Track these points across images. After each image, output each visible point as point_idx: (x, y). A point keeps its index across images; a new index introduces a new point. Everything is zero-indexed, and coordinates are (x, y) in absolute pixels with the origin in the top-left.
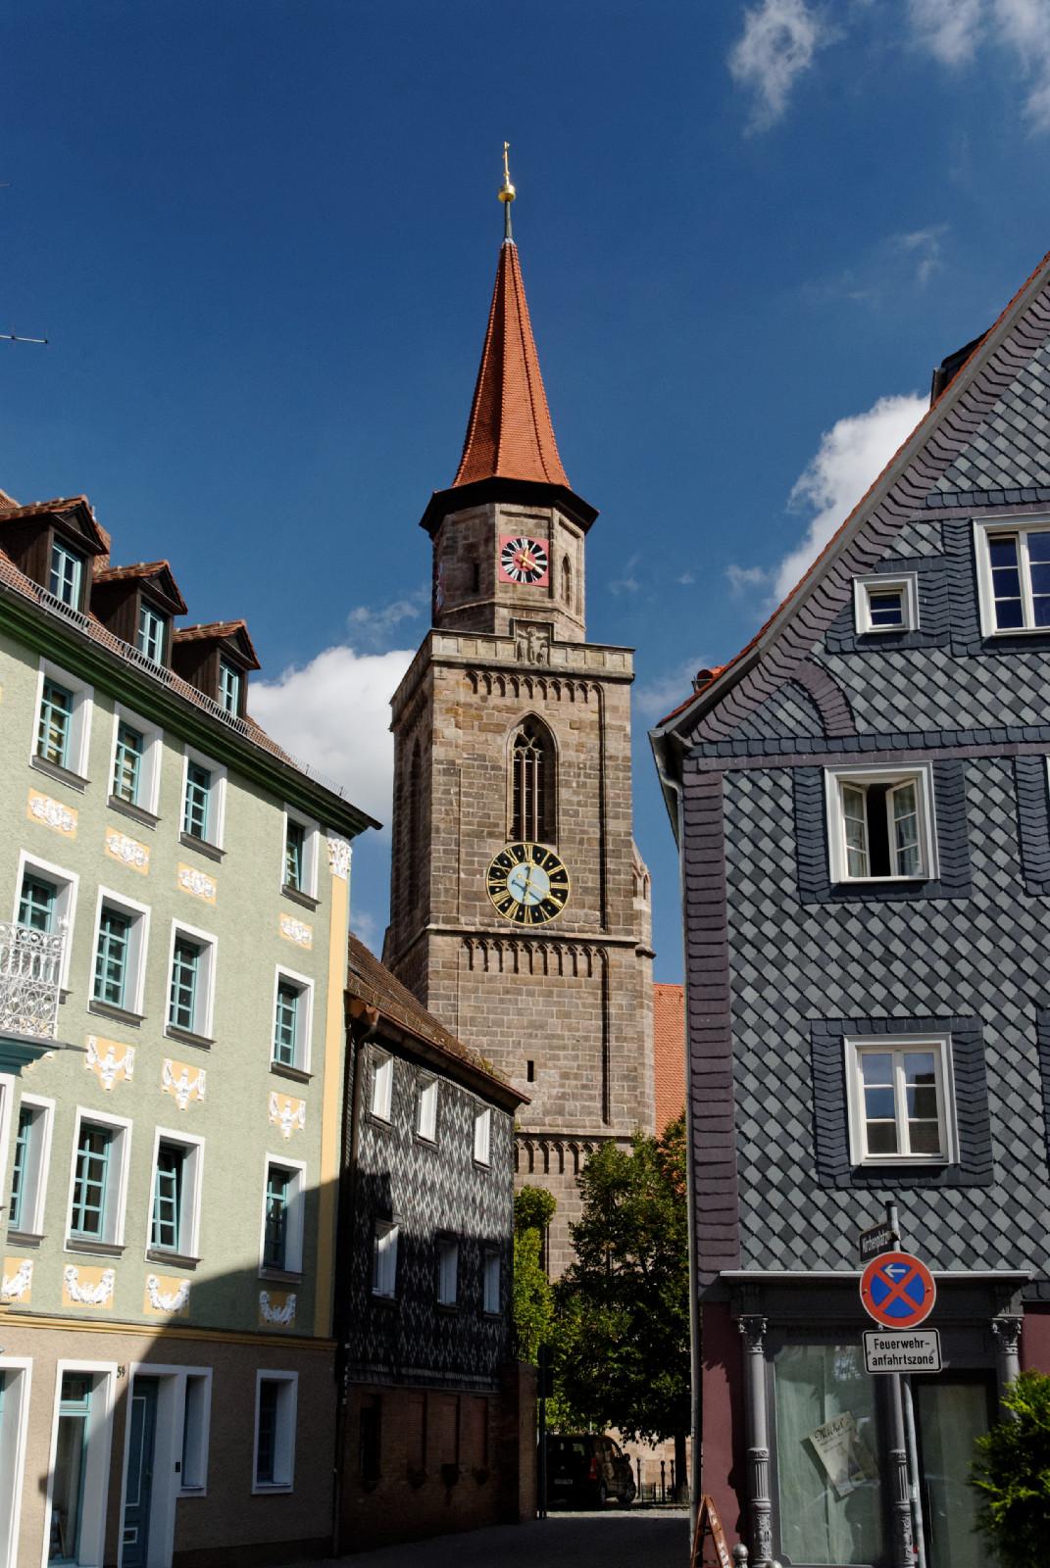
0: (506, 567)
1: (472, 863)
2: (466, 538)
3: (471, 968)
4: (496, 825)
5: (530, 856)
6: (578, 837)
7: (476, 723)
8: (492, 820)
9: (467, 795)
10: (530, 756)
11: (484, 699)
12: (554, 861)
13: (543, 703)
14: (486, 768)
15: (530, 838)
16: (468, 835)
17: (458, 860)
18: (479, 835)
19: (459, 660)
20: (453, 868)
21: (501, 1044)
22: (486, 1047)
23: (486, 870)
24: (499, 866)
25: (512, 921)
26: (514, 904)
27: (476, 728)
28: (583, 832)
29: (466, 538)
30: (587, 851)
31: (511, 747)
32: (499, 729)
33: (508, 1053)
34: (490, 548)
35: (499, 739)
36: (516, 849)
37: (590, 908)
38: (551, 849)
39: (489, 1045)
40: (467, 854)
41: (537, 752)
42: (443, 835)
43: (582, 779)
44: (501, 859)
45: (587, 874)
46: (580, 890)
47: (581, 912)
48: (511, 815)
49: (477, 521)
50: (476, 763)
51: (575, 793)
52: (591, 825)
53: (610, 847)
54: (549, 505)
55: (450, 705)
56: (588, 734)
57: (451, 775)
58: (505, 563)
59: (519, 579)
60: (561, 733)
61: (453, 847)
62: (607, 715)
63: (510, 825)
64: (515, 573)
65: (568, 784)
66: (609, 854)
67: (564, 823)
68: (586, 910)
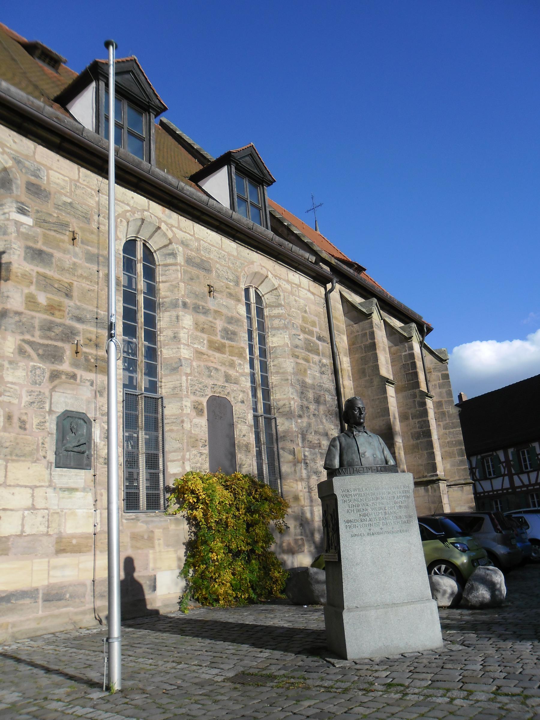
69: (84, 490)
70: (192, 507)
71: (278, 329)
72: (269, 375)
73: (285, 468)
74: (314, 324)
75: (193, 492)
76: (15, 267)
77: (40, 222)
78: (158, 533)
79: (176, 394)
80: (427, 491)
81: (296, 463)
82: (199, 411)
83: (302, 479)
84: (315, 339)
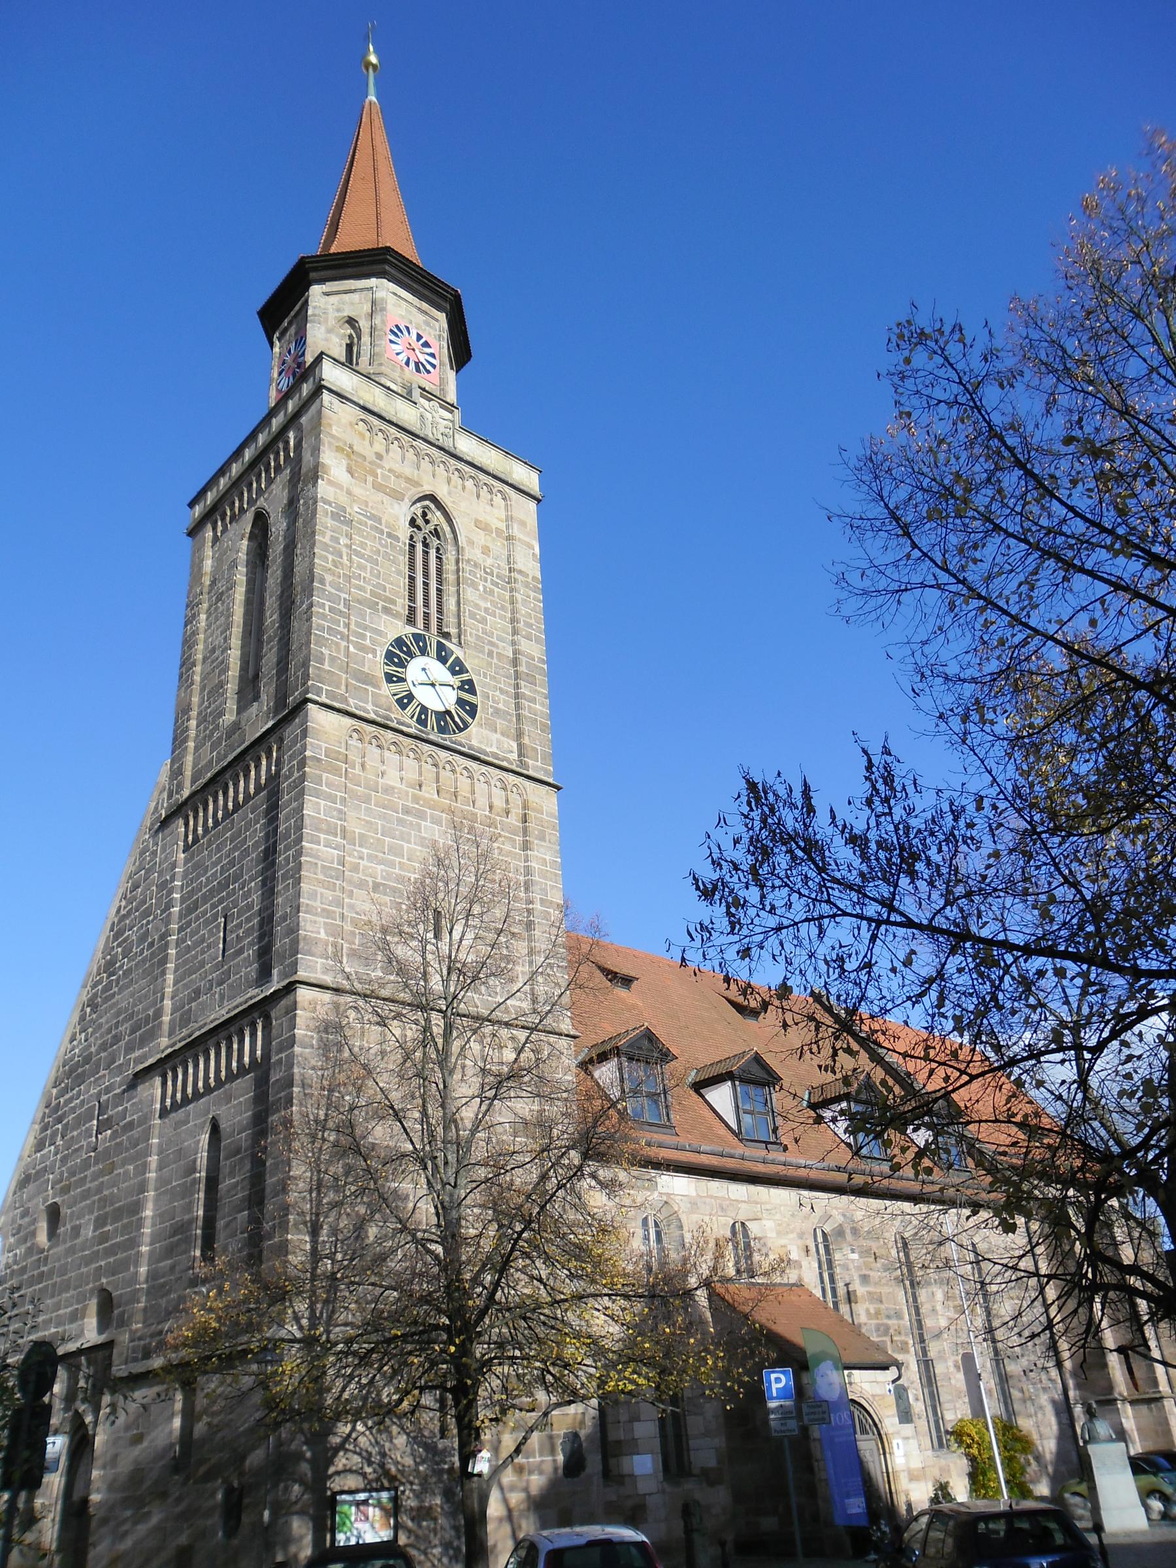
0: (393, 346)
1: (363, 637)
2: (338, 310)
3: (363, 765)
5: (433, 649)
8: (387, 594)
9: (358, 554)
12: (457, 668)
14: (382, 532)
17: (348, 626)
18: (373, 606)
19: (355, 399)
22: (379, 880)
23: (381, 653)
25: (413, 722)
26: (414, 703)
27: (369, 485)
28: (492, 644)
29: (338, 310)
32: (397, 496)
34: (377, 320)
35: (396, 506)
37: (503, 734)
39: (383, 878)
41: (435, 542)
43: (489, 585)
44: (399, 642)
45: (498, 693)
46: (491, 710)
49: (355, 297)
50: (370, 522)
51: (481, 597)
52: (500, 639)
53: (523, 669)
54: (439, 308)
55: (341, 444)
56: (494, 540)
57: (342, 522)
58: (391, 341)
59: (407, 363)
61: (341, 607)
64: (402, 358)
65: (474, 585)
66: (524, 676)
68: (498, 736)
69: (913, 1438)
70: (969, 1446)
73: (1017, 1406)
75: (969, 1435)
76: (859, 1294)
77: (861, 1253)
78: (952, 1466)
79: (942, 1357)
80: (1151, 1410)
81: (1024, 1401)
82: (958, 1368)
83: (1031, 1416)
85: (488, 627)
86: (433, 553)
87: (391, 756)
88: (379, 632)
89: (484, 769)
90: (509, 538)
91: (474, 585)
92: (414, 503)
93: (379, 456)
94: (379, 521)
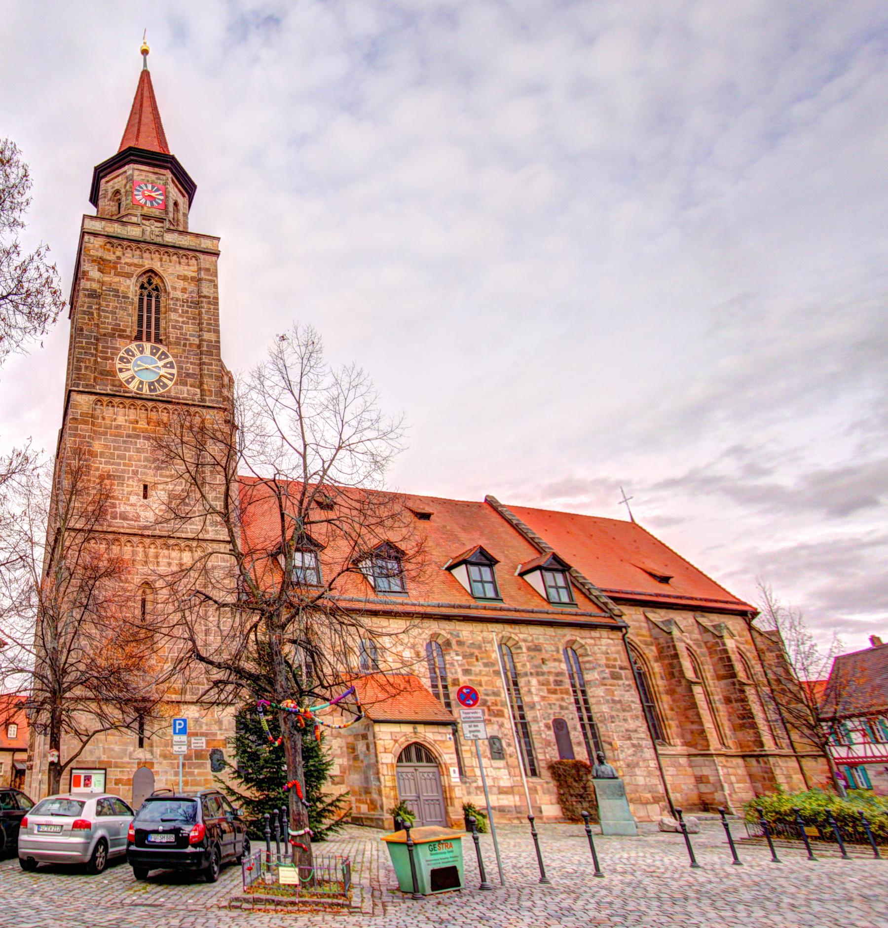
1: (106, 353)
4: (125, 331)
6: (182, 342)
7: (113, 271)
9: (104, 311)
10: (149, 296)
11: (119, 258)
13: (159, 264)
14: (119, 296)
15: (148, 340)
16: (105, 335)
17: (96, 349)
18: (112, 336)
20: (92, 355)
21: (124, 471)
24: (126, 356)
26: (136, 380)
30: (189, 351)
31: (137, 288)
32: (128, 276)
33: (129, 478)
35: (128, 281)
36: (138, 346)
38: (163, 348)
40: (103, 347)
41: (154, 293)
42: (85, 332)
43: (185, 308)
47: (185, 389)
48: (136, 328)
51: (180, 316)
52: (191, 335)
60: (170, 281)
61: (93, 340)
62: (202, 272)
63: (135, 334)
67: (173, 334)
71: (589, 669)
72: (588, 697)
74: (615, 660)
84: (617, 670)
85: (184, 331)
86: (153, 300)
87: (121, 411)
88: (117, 349)
89: (175, 407)
90: (200, 280)
91: (175, 311)
92: (141, 276)
93: (119, 258)
94: (117, 291)
